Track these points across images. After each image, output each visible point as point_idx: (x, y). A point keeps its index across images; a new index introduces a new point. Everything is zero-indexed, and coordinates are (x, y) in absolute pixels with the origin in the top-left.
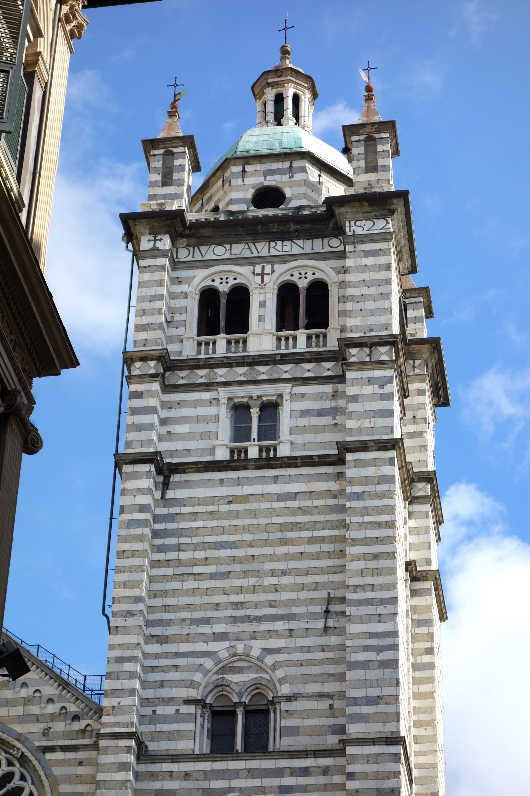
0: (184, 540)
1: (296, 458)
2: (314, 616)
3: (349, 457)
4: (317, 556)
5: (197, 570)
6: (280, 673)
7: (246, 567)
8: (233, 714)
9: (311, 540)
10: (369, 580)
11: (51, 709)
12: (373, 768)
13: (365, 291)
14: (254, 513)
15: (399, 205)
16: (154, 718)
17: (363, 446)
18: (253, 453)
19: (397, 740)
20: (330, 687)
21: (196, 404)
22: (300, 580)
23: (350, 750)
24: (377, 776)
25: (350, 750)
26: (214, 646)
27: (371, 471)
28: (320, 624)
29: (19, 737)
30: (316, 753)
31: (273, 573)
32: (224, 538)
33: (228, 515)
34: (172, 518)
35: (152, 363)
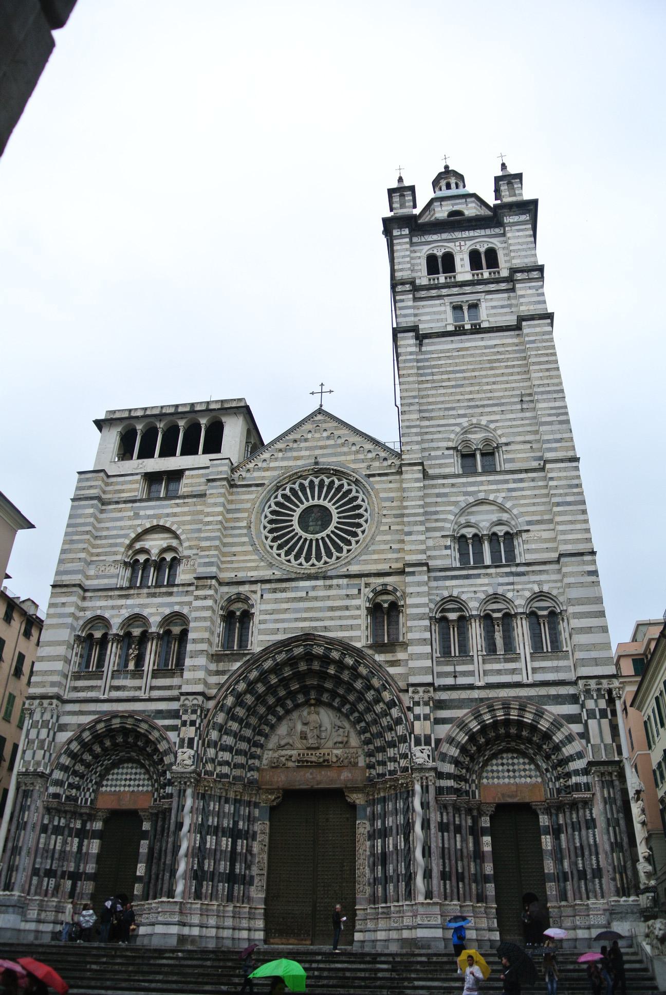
0: (434, 370)
2: (515, 403)
3: (524, 323)
4: (512, 374)
5: (444, 384)
6: (499, 432)
7: (473, 381)
8: (473, 456)
9: (507, 367)
10: (546, 382)
11: (370, 456)
12: (564, 474)
13: (520, 247)
14: (472, 355)
16: (430, 457)
17: (532, 318)
18: (468, 327)
19: (577, 460)
20: (528, 438)
21: (432, 306)
22: (503, 386)
23: (548, 466)
24: (566, 478)
25: (548, 466)
26: (459, 421)
27: (538, 330)
28: (519, 407)
30: (527, 471)
31: (487, 384)
34: (427, 360)
35: (408, 286)
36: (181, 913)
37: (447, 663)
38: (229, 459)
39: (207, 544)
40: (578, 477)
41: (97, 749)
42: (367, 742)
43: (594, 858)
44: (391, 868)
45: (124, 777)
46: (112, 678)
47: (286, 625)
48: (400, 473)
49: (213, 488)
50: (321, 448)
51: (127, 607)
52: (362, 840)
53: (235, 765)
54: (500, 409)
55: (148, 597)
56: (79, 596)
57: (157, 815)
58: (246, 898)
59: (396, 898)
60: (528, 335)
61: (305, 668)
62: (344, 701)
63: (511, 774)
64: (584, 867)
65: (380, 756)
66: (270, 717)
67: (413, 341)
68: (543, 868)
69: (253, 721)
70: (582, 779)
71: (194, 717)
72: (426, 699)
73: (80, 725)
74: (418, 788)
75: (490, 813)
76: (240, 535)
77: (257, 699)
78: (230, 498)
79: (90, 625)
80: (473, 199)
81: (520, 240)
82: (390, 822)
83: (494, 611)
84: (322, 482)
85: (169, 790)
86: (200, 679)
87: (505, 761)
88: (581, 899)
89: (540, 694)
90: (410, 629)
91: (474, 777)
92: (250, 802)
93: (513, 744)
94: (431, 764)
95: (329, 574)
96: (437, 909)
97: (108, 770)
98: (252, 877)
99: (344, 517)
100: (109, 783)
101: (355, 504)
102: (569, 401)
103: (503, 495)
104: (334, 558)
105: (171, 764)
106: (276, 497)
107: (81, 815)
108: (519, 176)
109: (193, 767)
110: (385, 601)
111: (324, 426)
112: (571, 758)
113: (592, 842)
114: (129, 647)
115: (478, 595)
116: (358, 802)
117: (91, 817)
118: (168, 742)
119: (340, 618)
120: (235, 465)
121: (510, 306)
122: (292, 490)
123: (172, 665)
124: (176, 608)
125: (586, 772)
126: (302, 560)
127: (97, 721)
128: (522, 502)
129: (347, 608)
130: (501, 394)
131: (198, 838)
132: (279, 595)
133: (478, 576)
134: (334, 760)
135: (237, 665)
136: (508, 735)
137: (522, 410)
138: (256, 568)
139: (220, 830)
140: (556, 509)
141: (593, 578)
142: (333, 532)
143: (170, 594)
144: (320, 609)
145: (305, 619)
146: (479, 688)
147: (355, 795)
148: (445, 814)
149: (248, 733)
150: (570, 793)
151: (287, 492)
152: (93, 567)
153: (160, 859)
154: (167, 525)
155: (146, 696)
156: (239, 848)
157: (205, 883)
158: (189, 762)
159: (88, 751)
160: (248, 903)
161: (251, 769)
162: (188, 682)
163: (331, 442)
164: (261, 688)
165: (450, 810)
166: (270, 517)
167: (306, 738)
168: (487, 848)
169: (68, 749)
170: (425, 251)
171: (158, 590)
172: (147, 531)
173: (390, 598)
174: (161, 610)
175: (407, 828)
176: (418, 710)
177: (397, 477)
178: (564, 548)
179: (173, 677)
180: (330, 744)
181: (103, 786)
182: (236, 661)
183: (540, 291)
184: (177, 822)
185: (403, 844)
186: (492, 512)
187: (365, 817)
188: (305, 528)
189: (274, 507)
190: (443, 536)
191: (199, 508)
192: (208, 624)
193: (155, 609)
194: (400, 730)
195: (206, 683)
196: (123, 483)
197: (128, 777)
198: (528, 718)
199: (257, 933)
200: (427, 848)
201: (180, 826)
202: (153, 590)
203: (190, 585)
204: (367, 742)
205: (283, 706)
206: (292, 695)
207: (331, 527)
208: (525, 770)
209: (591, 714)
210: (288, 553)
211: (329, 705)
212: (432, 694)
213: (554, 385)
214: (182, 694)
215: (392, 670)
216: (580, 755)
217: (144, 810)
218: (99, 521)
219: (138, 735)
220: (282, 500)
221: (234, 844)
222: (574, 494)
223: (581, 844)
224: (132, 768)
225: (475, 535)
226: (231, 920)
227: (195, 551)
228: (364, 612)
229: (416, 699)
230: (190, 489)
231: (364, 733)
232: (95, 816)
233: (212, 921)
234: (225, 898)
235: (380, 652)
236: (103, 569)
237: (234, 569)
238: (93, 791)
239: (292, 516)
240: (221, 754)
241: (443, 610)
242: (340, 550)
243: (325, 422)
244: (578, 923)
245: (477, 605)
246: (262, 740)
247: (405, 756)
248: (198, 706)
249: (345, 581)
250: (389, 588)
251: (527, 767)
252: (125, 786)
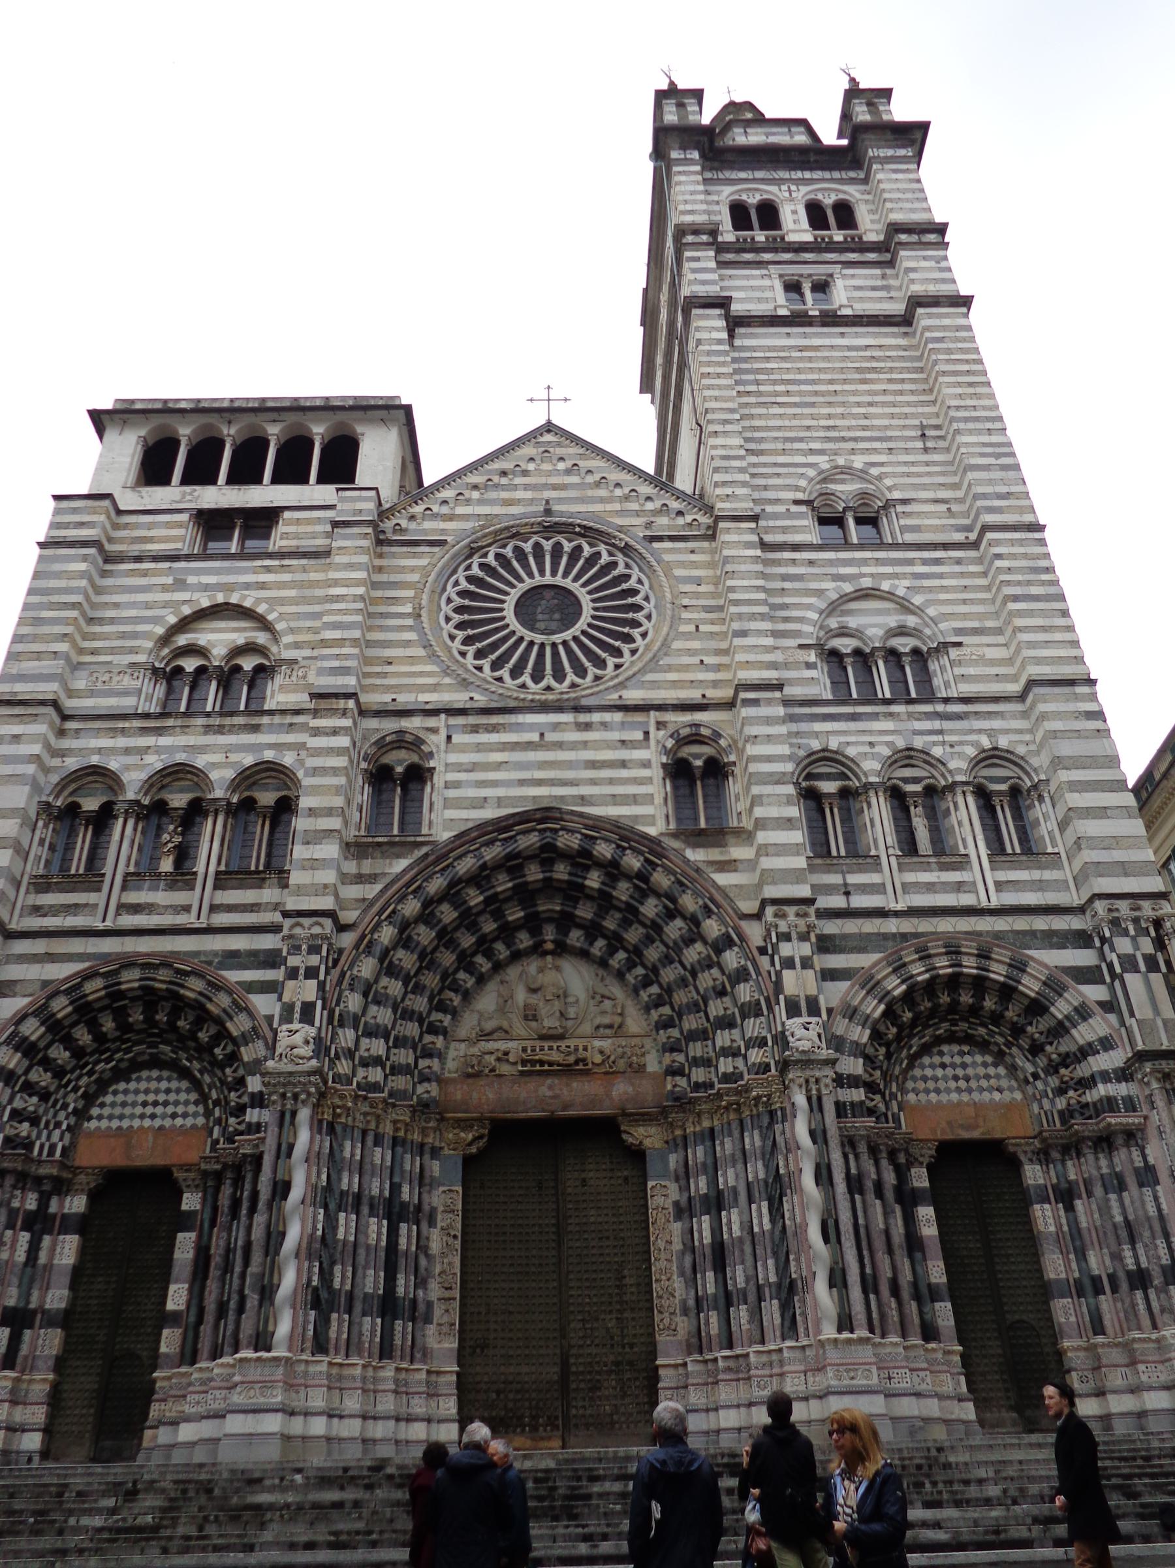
1: (861, 316)
2: (912, 439)
3: (920, 311)
4: (901, 393)
5: (779, 400)
8: (839, 522)
9: (890, 381)
10: (969, 402)
11: (650, 506)
12: (1022, 550)
15: (918, 135)
17: (934, 301)
19: (1041, 528)
21: (747, 277)
24: (1025, 556)
27: (947, 322)
29: (621, 529)
30: (945, 546)
31: (859, 404)
32: (803, 377)
33: (801, 359)
36: (289, 1386)
37: (829, 869)
38: (376, 489)
39: (337, 634)
40: (1047, 556)
41: (83, 1036)
42: (666, 1024)
43: (1161, 1243)
44: (739, 1276)
45: (141, 1098)
46: (124, 888)
47: (501, 792)
48: (713, 537)
49: (345, 537)
50: (555, 487)
51: (158, 750)
52: (661, 1221)
53: (393, 1067)
54: (885, 445)
55: (206, 733)
56: (51, 724)
57: (218, 1176)
58: (417, 1351)
59: (758, 1337)
60: (928, 329)
61: (541, 876)
62: (615, 942)
63: (962, 1084)
64: (1138, 1263)
65: (696, 1049)
66: (461, 975)
67: (722, 323)
68: (1040, 1271)
69: (431, 980)
70: (1121, 1090)
71: (314, 960)
72: (803, 928)
73: (45, 983)
74: (800, 1099)
75: (926, 1161)
76: (401, 628)
77: (441, 935)
78: (377, 562)
79: (73, 786)
80: (802, 129)
81: (899, 186)
82: (729, 1178)
83: (906, 780)
84: (557, 550)
85: (252, 1115)
86: (325, 886)
87: (947, 1059)
88: (1140, 1328)
89: (1016, 927)
90: (756, 801)
91: (894, 1089)
92: (422, 1145)
93: (964, 1026)
94: (825, 1053)
95: (584, 702)
96: (866, 1353)
97: (103, 1086)
98: (429, 1305)
99: (605, 609)
100: (106, 1111)
101: (624, 586)
102: (1014, 433)
103: (907, 583)
104: (590, 677)
105: (258, 1062)
106: (469, 568)
107: (38, 1180)
108: (887, 93)
109: (314, 1062)
110: (697, 756)
111: (560, 451)
112: (1086, 1051)
113: (1152, 1210)
114: (160, 830)
115: (877, 749)
116: (647, 1143)
117: (61, 1187)
118: (251, 1015)
119: (611, 781)
120: (386, 506)
121: (887, 288)
122: (498, 556)
123: (256, 860)
124: (269, 755)
125: (1124, 1074)
126: (526, 678)
127: (87, 976)
128: (943, 596)
129: (623, 764)
130: (886, 422)
131: (321, 1217)
132: (484, 738)
133: (875, 716)
134: (598, 1059)
135: (400, 865)
136: (954, 1007)
137: (926, 450)
138: (435, 688)
139: (365, 1200)
140: (1012, 606)
141: (1098, 724)
142: (583, 632)
143: (256, 728)
144: (569, 765)
145: (540, 783)
146: (897, 914)
147: (641, 1130)
148: (851, 1157)
149: (420, 1003)
150: (1090, 1118)
151: (490, 559)
152: (84, 674)
153: (227, 1267)
154: (247, 604)
155: (203, 923)
156: (403, 1242)
157: (334, 1316)
158: (306, 1051)
159: (61, 1041)
160: (424, 1360)
161: (424, 1079)
162: (300, 891)
163: (574, 479)
164: (447, 914)
165: (862, 1148)
166: (458, 601)
167: (535, 1018)
168: (929, 1230)
169: (14, 1034)
170: (726, 193)
171: (228, 721)
172: (202, 615)
173: (707, 750)
174: (234, 757)
175: (777, 1189)
176: (786, 949)
177: (706, 544)
178: (1035, 671)
179: (260, 887)
180: (587, 1028)
181: (90, 1118)
182: (398, 856)
183: (943, 264)
184: (275, 1184)
185: (766, 1220)
186: (886, 612)
187: (664, 1176)
188: (530, 625)
189: (464, 585)
190: (801, 646)
191: (314, 576)
192: (342, 780)
193: (220, 756)
194: (745, 993)
195: (336, 895)
196: (150, 526)
197: (151, 1098)
198: (998, 972)
199: (443, 1427)
200: (831, 1222)
201: (282, 1189)
202: (218, 721)
203: (297, 712)
204: (666, 1024)
205: (489, 954)
206: (507, 932)
207: (582, 624)
208: (987, 1077)
209: (1129, 963)
210: (496, 666)
211: (584, 954)
212: (812, 918)
213: (984, 408)
214: (286, 914)
215: (722, 879)
216: (1107, 1044)
217: (187, 1167)
218: (99, 591)
219: (178, 1003)
220: (481, 574)
221: (393, 1233)
222: (1043, 583)
223: (1126, 1218)
224: (159, 1079)
225: (857, 652)
226: (391, 1397)
227: (307, 653)
228: (657, 773)
229: (783, 927)
230: (294, 543)
231: (657, 1006)
232: (70, 1182)
233: (352, 1403)
234: (376, 1350)
235: (695, 846)
236: (106, 677)
237: (388, 688)
238: (69, 1128)
239: (503, 602)
240: (365, 1042)
241: (809, 777)
242: (601, 664)
243: (559, 445)
244: (1144, 1378)
245: (877, 766)
246: (447, 1020)
247: (762, 1043)
248: (325, 938)
249: (618, 717)
250: (704, 731)
251: (991, 1071)
252: (142, 1116)
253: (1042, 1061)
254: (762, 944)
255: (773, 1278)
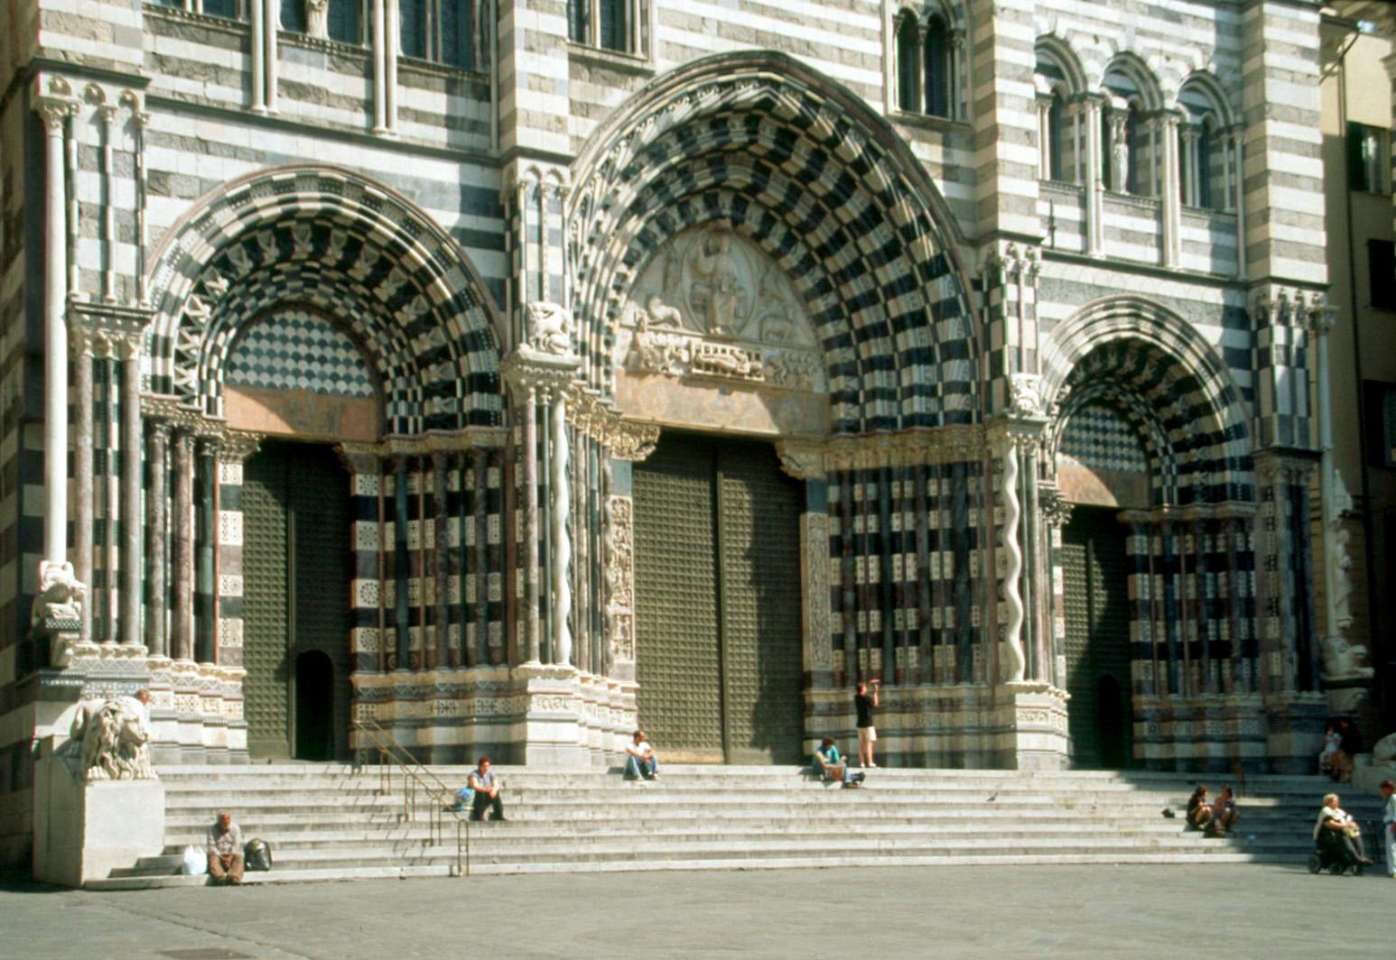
63: (1100, 449)
68: (1127, 632)
85: (476, 401)
87: (1091, 422)
94: (1040, 415)
119: (839, 28)
127: (262, 184)
135: (615, 96)
169: (177, 250)
182: (612, 83)
194: (951, 330)
198: (1168, 343)
212: (1039, 261)
235: (922, 139)
247: (965, 388)
251: (1125, 439)
253: (1175, 436)
254: (975, 276)
255: (950, 625)
